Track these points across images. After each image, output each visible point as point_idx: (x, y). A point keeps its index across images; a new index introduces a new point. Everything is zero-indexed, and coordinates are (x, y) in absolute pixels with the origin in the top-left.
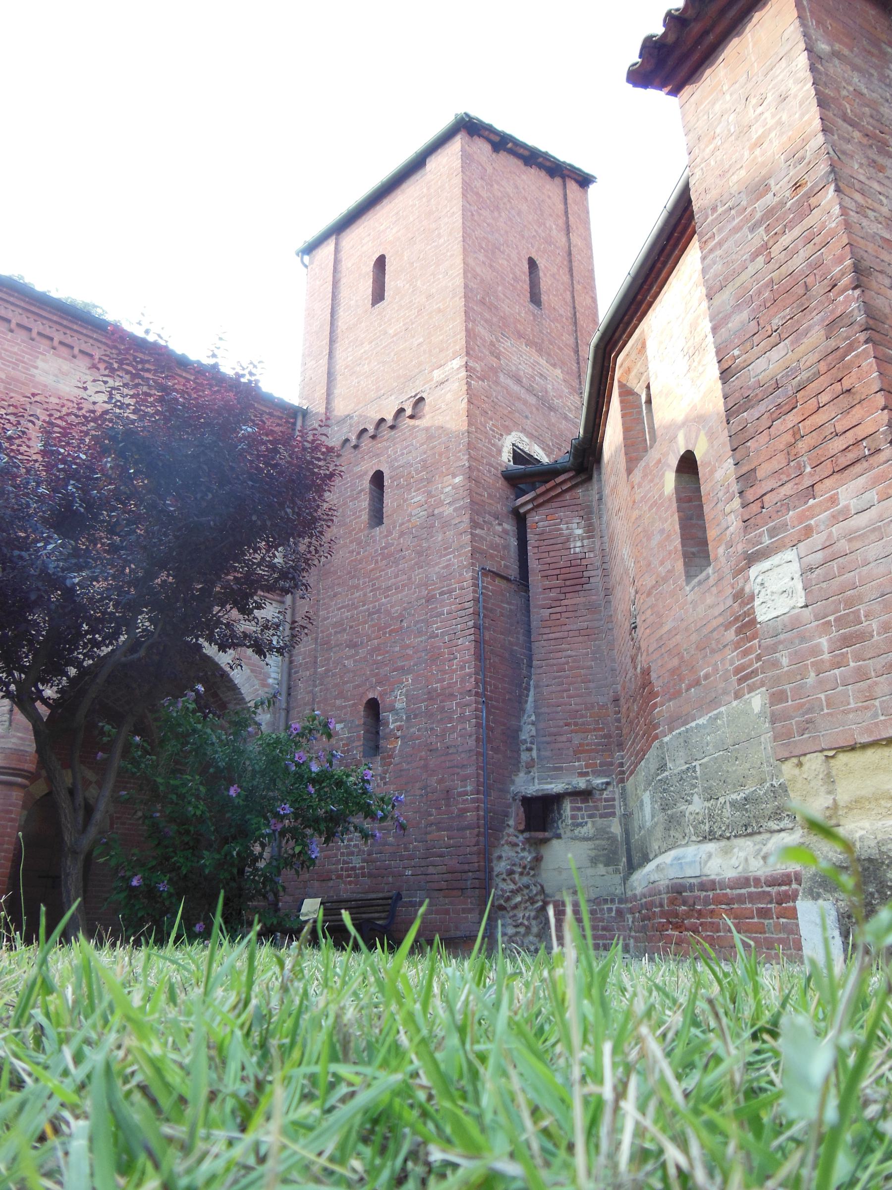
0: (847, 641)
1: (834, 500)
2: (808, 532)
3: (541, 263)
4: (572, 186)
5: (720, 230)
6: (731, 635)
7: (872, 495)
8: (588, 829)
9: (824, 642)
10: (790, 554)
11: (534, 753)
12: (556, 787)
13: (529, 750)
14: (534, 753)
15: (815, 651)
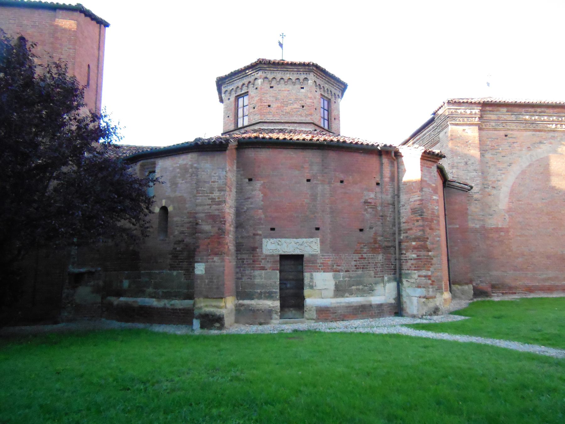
0: (211, 282)
1: (213, 259)
2: (207, 262)
3: (91, 66)
4: (102, 26)
5: (202, 193)
6: (170, 256)
7: (220, 261)
8: (92, 283)
9: (207, 281)
10: (203, 264)
11: (76, 259)
12: (83, 270)
13: (74, 258)
14: (76, 259)
15: (205, 282)
